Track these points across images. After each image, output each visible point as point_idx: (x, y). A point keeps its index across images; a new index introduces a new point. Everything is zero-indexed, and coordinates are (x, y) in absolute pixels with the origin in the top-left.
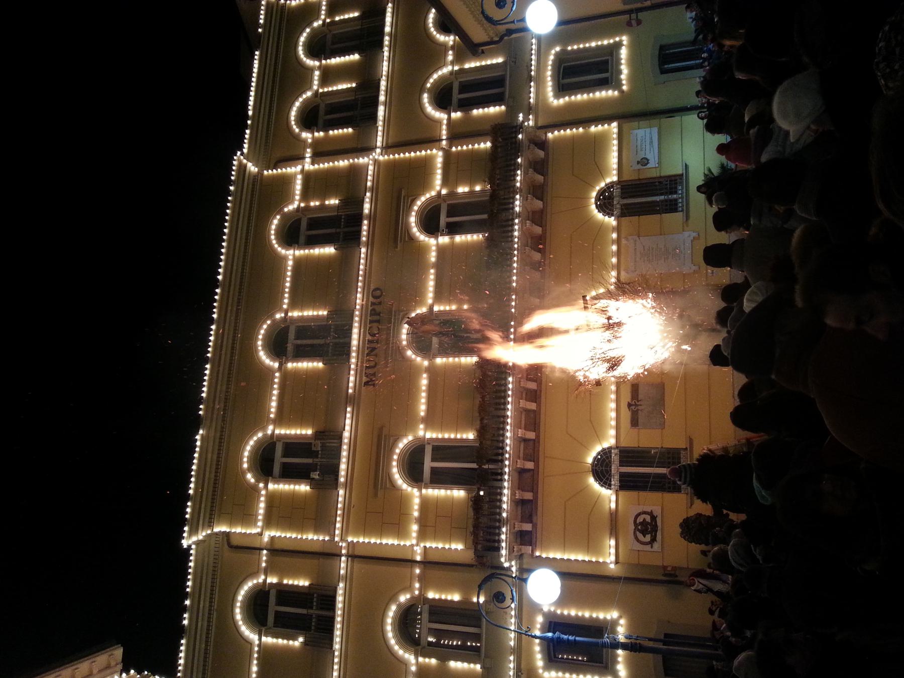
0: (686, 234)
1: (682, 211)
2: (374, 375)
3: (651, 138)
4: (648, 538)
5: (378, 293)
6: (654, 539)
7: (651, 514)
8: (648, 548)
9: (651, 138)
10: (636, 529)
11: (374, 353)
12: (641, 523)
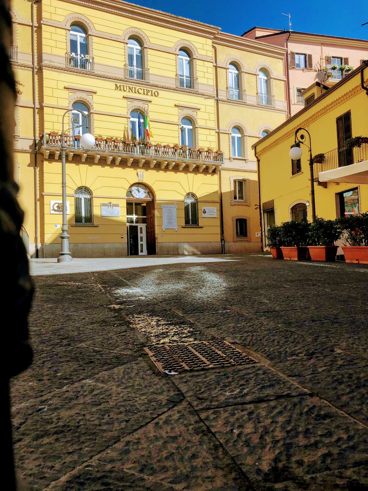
4: (56, 208)
5: (156, 94)
6: (55, 210)
8: (52, 208)
11: (130, 90)
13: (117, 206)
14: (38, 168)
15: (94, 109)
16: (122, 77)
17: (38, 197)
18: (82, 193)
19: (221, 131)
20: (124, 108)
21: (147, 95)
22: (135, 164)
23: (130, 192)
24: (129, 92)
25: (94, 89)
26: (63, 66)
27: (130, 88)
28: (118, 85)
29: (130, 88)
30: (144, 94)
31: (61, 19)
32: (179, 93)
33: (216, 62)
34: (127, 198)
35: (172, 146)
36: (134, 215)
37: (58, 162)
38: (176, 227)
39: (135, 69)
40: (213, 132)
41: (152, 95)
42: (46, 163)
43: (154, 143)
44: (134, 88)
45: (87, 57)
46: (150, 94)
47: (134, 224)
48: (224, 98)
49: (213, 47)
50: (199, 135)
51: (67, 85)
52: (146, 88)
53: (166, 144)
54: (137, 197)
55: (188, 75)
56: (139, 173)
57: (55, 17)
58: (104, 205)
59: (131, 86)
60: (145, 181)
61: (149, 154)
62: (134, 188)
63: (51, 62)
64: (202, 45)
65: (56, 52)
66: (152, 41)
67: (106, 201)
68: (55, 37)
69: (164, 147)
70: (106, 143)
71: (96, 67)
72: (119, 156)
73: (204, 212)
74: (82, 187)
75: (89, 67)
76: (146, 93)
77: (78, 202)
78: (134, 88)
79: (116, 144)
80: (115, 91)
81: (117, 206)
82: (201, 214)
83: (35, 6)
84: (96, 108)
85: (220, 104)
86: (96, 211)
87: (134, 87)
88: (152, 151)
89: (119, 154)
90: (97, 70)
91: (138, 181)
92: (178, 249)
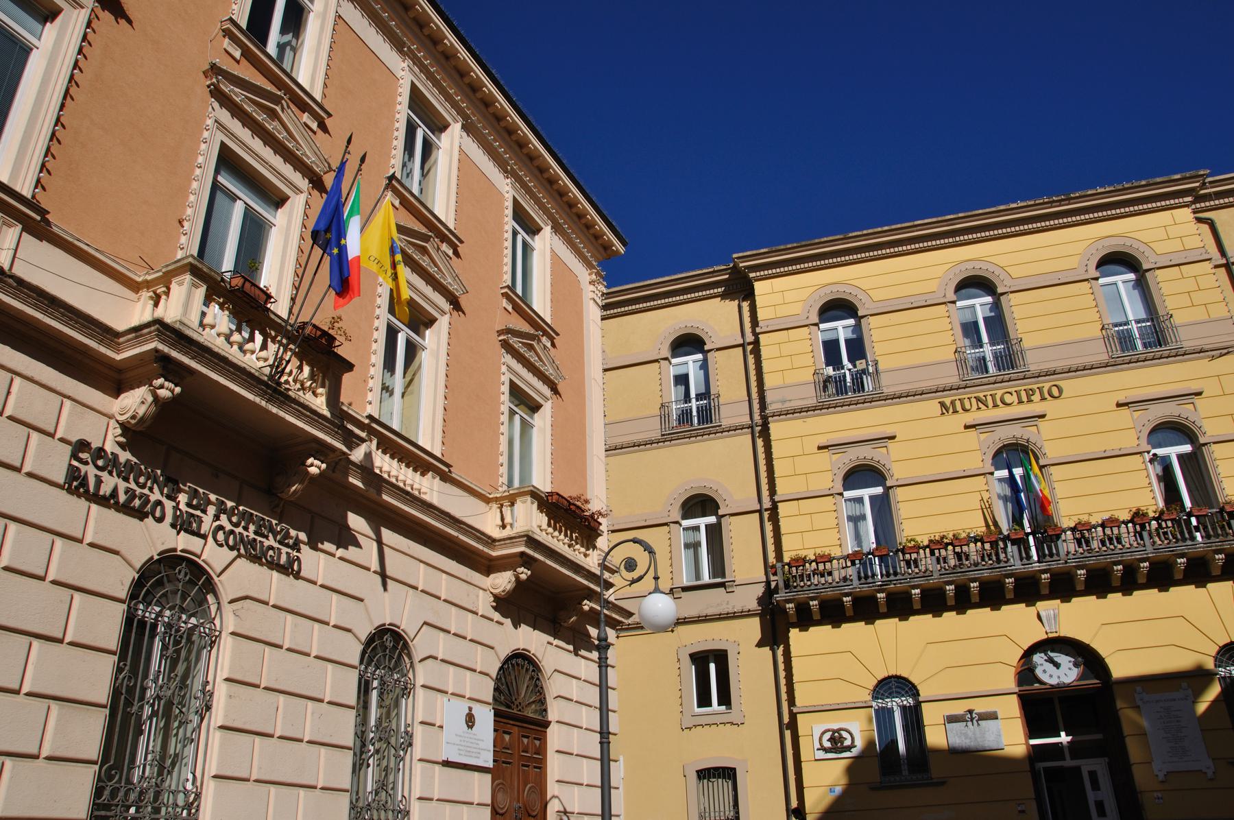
2: (955, 412)
5: (1055, 392)
6: (826, 750)
8: (817, 745)
10: (834, 731)
12: (841, 737)
13: (993, 716)
14: (781, 648)
15: (895, 477)
16: (954, 380)
17: (786, 719)
18: (891, 695)
21: (1030, 401)
23: (1026, 674)
24: (979, 408)
25: (889, 431)
26: (812, 402)
27: (978, 399)
28: (948, 401)
29: (978, 399)
30: (1020, 402)
32: (1122, 370)
33: (1223, 253)
34: (1017, 690)
35: (1125, 516)
36: (1063, 734)
39: (988, 350)
41: (1043, 399)
42: (794, 633)
43: (1066, 523)
44: (989, 398)
45: (861, 364)
46: (1037, 397)
47: (1069, 763)
49: (1199, 220)
50: (1218, 462)
51: (823, 441)
52: (1022, 386)
53: (1106, 516)
54: (1054, 681)
55: (1143, 315)
56: (1043, 614)
58: (952, 719)
59: (981, 395)
60: (1066, 631)
61: (1058, 554)
62: (1038, 658)
63: (784, 402)
64: (1163, 231)
66: (1015, 272)
67: (959, 708)
69: (1103, 525)
70: (932, 553)
71: (885, 379)
72: (974, 580)
74: (889, 677)
75: (868, 383)
76: (1024, 398)
77: (884, 717)
78: (989, 398)
79: (958, 549)
80: (944, 418)
81: (993, 716)
83: (745, 305)
84: (897, 472)
86: (936, 737)
88: (1068, 545)
89: (972, 575)
90: (889, 384)
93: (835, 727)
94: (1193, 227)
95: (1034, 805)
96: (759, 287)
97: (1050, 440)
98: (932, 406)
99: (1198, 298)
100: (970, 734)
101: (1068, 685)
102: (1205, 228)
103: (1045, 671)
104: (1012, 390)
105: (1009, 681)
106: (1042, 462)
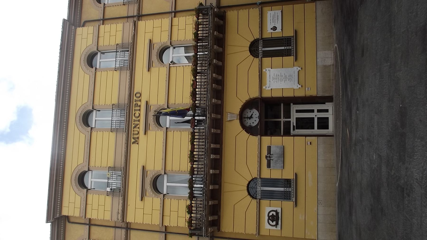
0: (295, 68)
1: (293, 55)
3: (278, 16)
4: (274, 223)
6: (277, 224)
7: (276, 211)
8: (274, 228)
9: (278, 16)
11: (138, 127)
13: (269, 148)
19: (173, 10)
20: (156, 135)
21: (140, 106)
22: (218, 124)
24: (138, 128)
27: (135, 127)
28: (133, 140)
29: (135, 127)
30: (140, 110)
31: (78, 198)
37: (220, 216)
38: (296, 69)
40: (175, 20)
48: (136, 7)
54: (258, 120)
57: (78, 204)
58: (269, 166)
59: (133, 126)
60: (237, 111)
63: (118, 213)
65: (108, 207)
67: (265, 162)
68: (95, 206)
73: (275, 28)
76: (138, 108)
81: (269, 148)
82: (278, 33)
84: (159, 168)
85: (143, 13)
87: (133, 122)
91: (238, 122)
92: (325, 67)
93: (267, 218)
94: (85, 29)
95: (308, 138)
96: (65, 212)
97: (158, 101)
98: (134, 147)
99: (113, 33)
100: (276, 159)
101: (260, 114)
102: (87, 24)
103: (253, 123)
104: (134, 112)
105: (255, 139)
106: (166, 107)
